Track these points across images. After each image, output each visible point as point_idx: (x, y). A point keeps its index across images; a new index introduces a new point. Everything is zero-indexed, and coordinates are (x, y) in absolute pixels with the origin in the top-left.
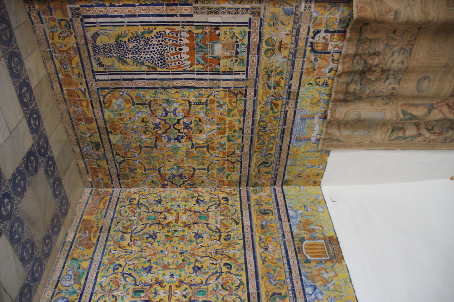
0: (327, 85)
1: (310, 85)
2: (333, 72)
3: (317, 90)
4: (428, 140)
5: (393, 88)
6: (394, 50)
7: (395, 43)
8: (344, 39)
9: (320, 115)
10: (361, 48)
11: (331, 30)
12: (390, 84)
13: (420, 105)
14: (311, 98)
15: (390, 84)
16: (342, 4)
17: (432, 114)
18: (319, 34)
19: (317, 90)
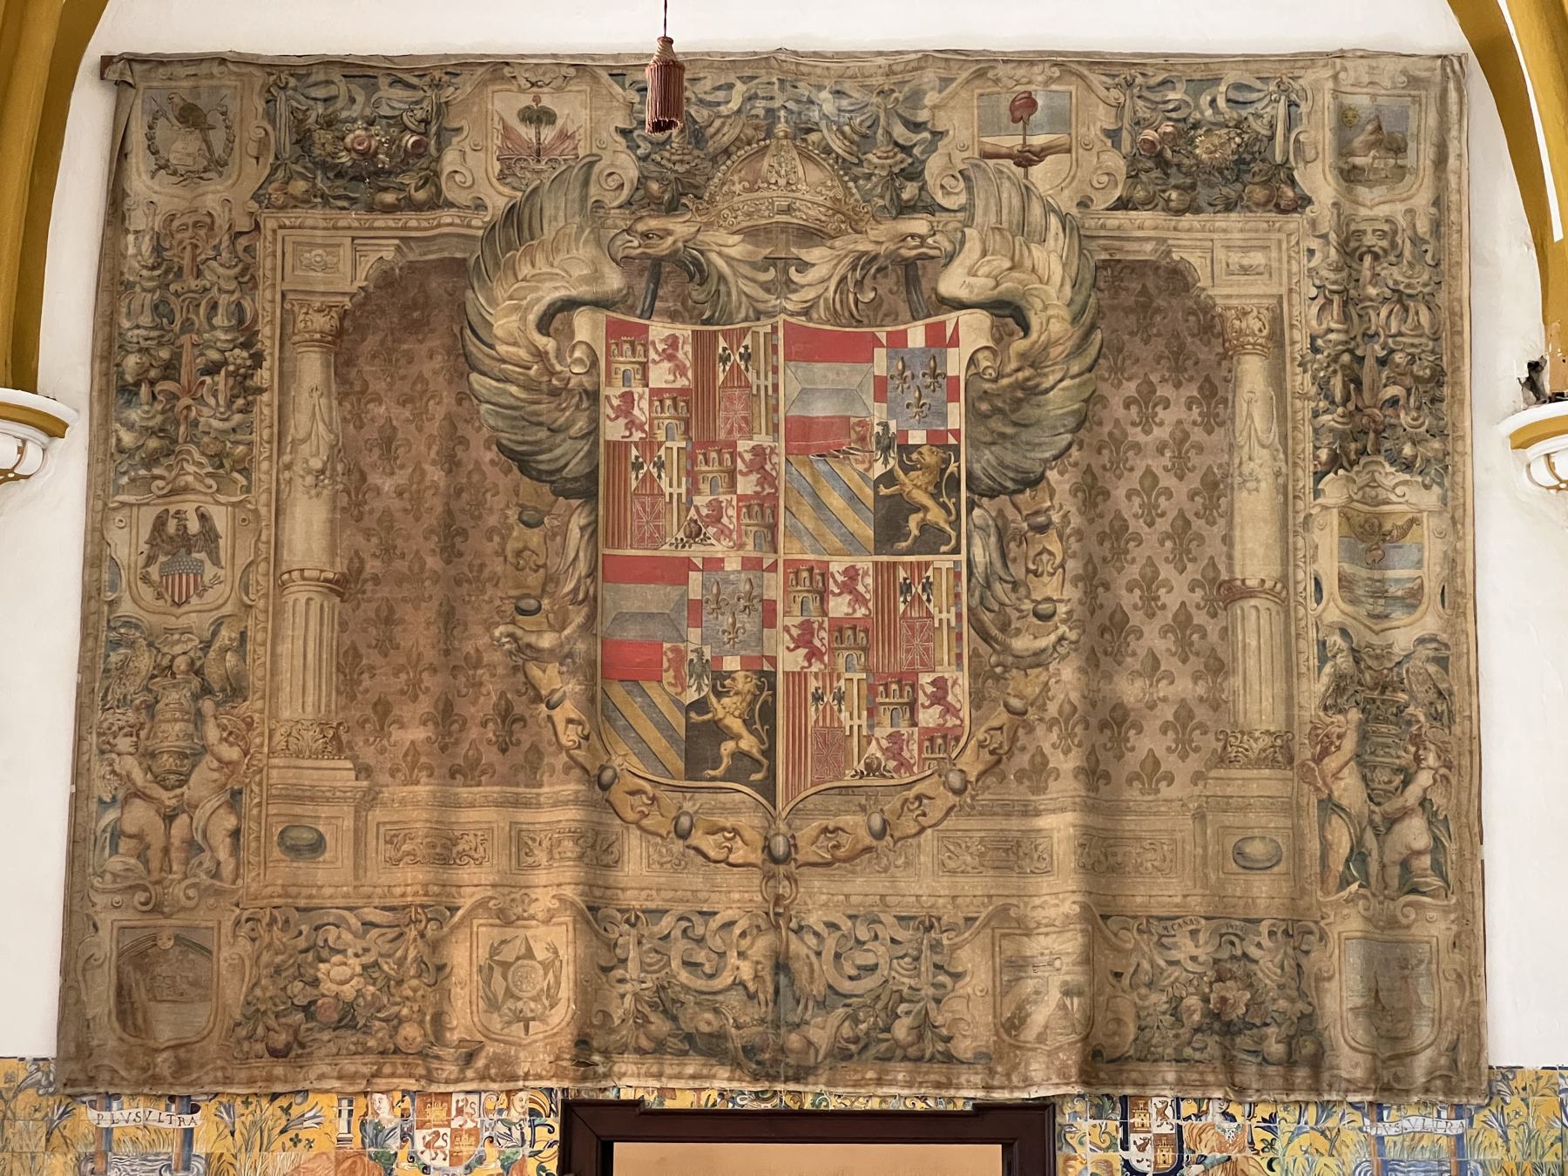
0: (1273, 1118)
1: (1274, 1165)
2: (1234, 1109)
3: (1290, 1141)
4: (1443, 771)
5: (1271, 934)
6: (1162, 963)
7: (1146, 965)
8: (1140, 1097)
9: (1367, 1122)
10: (1160, 1050)
11: (1121, 1135)
12: (1259, 945)
13: (1323, 838)
15: (1259, 945)
16: (1059, 1119)
17: (1345, 803)
18: (1134, 1163)
19: (1290, 1141)
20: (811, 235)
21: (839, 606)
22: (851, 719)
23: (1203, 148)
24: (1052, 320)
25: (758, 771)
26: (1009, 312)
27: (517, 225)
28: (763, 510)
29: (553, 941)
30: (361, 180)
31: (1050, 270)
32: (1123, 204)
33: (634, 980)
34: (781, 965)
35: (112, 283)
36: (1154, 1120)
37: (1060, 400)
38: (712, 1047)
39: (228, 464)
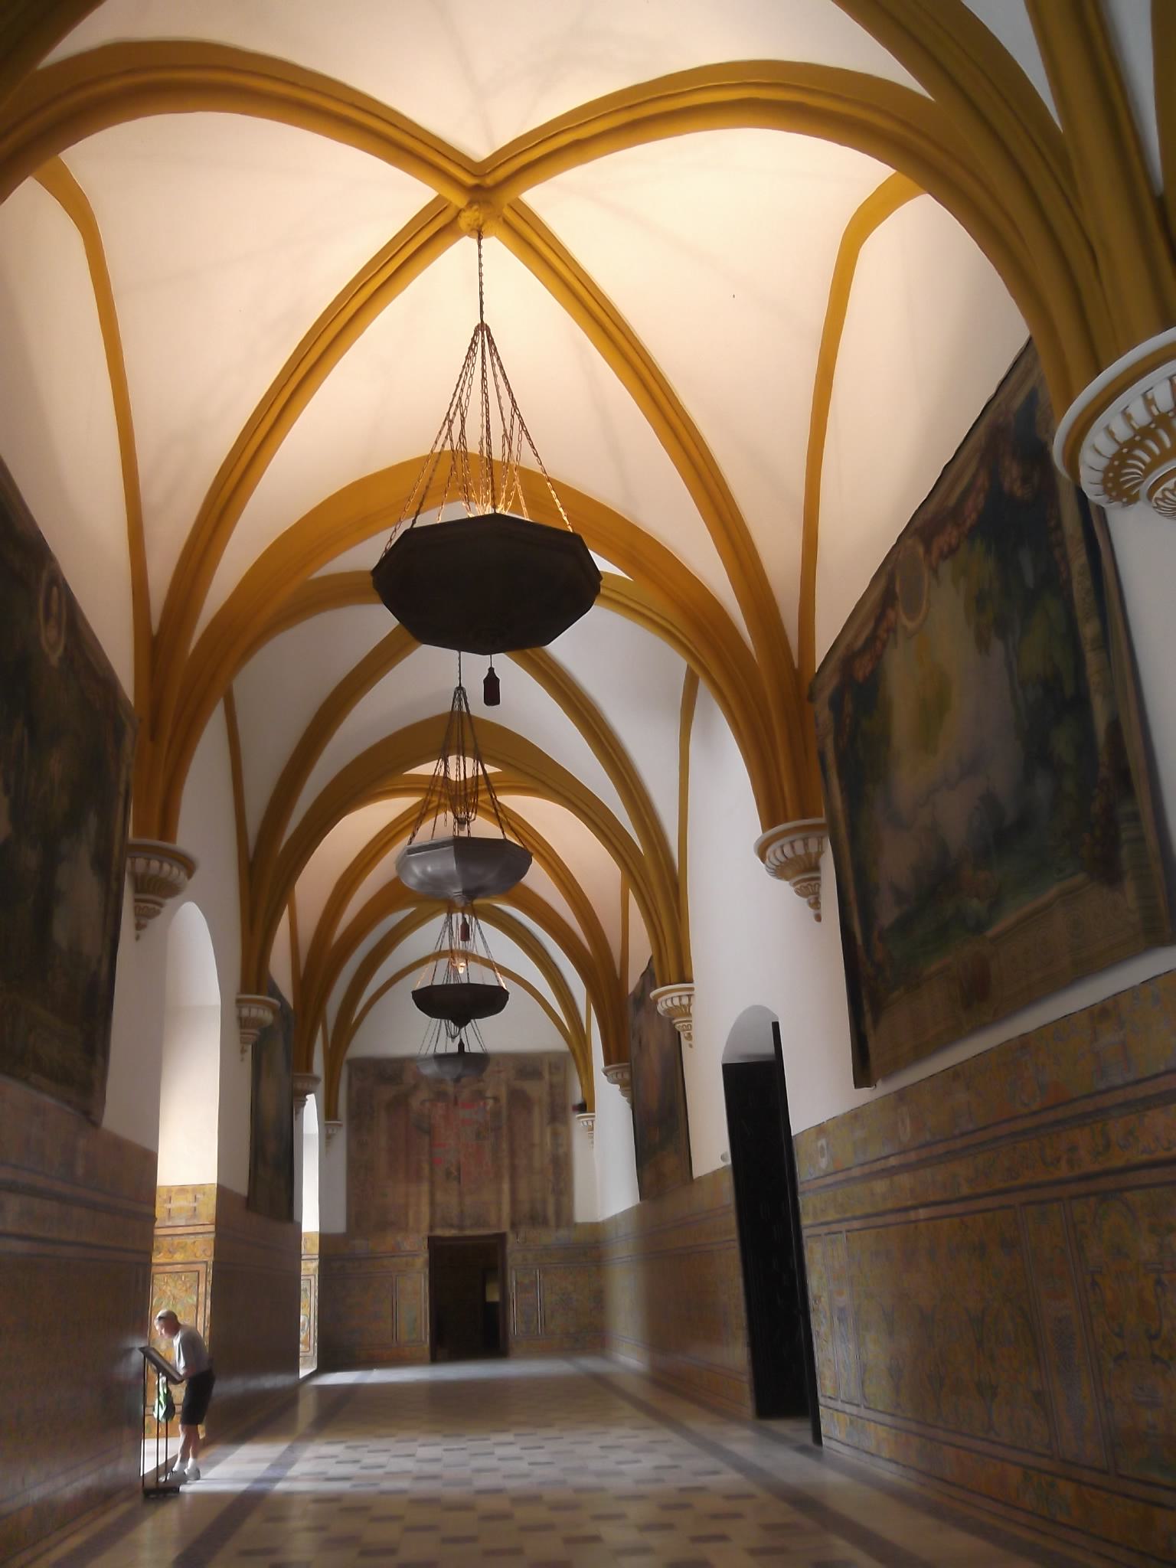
14: (549, 1237)
24: (504, 1100)
26: (496, 1099)
31: (503, 1093)
35: (350, 1100)
36: (522, 1235)
38: (452, 1226)
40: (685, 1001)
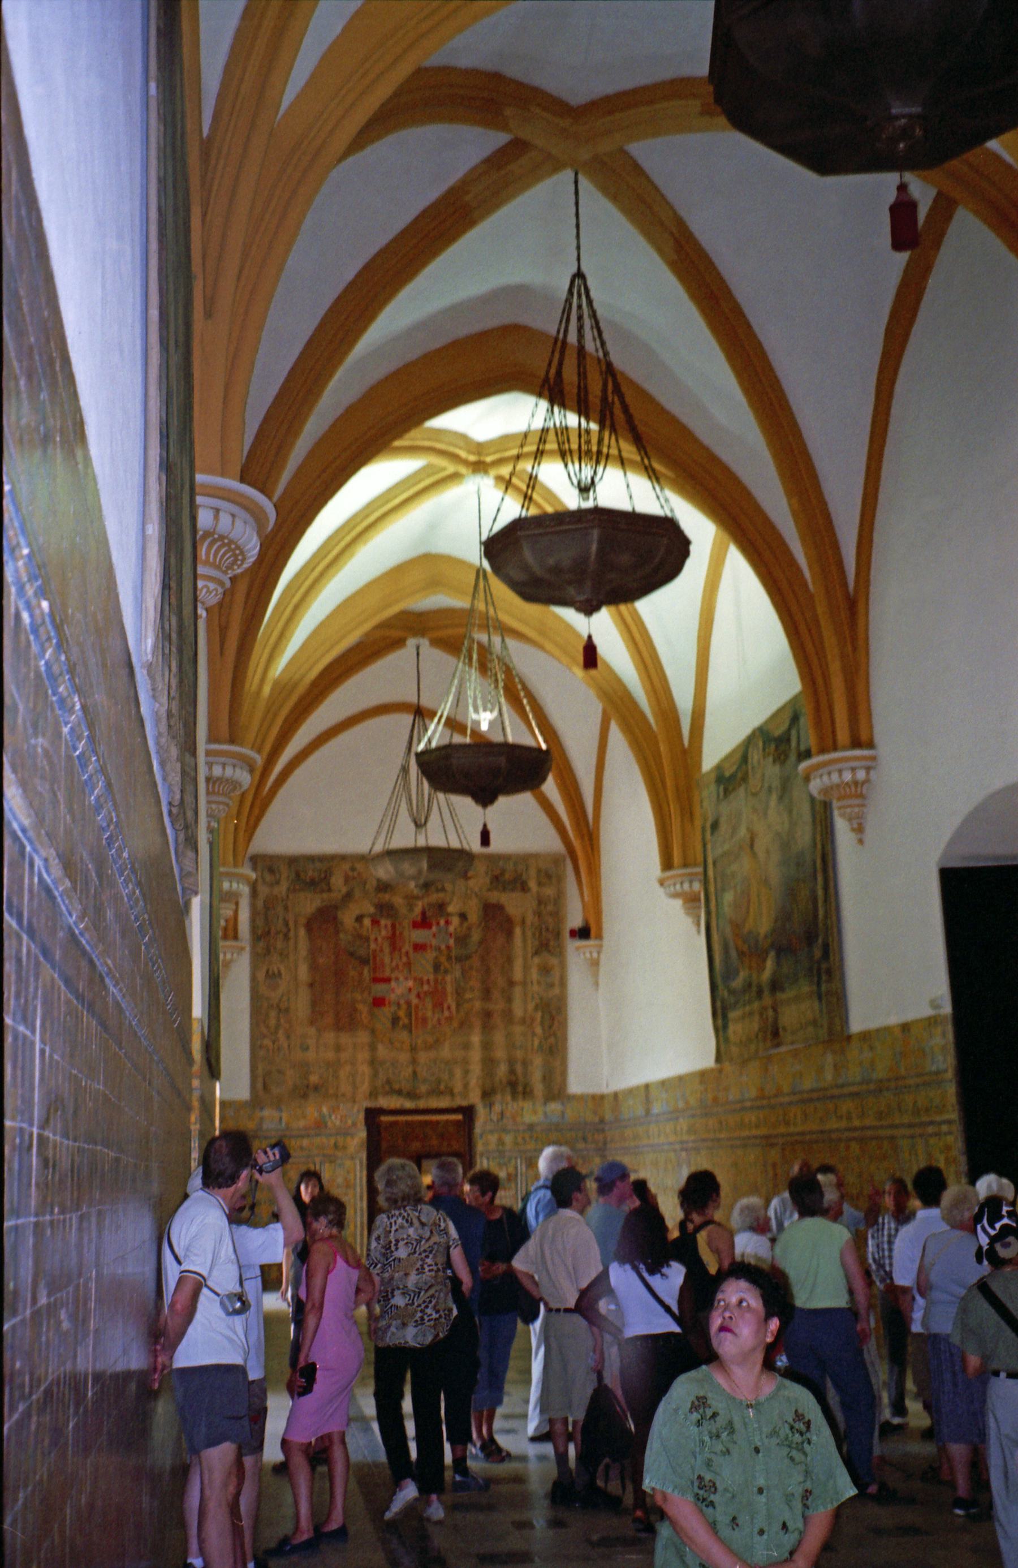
14: (532, 1113)
20: (417, 898)
21: (426, 988)
22: (429, 1014)
23: (507, 876)
24: (474, 917)
25: (409, 1028)
26: (463, 916)
27: (348, 896)
28: (408, 965)
29: (365, 1069)
30: (313, 884)
32: (489, 890)
33: (382, 1077)
34: (415, 1073)
36: (497, 1108)
37: (476, 936)
38: (399, 1093)
39: (284, 955)
40: (861, 775)
